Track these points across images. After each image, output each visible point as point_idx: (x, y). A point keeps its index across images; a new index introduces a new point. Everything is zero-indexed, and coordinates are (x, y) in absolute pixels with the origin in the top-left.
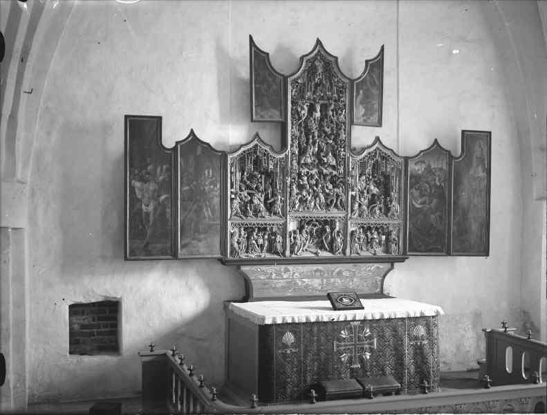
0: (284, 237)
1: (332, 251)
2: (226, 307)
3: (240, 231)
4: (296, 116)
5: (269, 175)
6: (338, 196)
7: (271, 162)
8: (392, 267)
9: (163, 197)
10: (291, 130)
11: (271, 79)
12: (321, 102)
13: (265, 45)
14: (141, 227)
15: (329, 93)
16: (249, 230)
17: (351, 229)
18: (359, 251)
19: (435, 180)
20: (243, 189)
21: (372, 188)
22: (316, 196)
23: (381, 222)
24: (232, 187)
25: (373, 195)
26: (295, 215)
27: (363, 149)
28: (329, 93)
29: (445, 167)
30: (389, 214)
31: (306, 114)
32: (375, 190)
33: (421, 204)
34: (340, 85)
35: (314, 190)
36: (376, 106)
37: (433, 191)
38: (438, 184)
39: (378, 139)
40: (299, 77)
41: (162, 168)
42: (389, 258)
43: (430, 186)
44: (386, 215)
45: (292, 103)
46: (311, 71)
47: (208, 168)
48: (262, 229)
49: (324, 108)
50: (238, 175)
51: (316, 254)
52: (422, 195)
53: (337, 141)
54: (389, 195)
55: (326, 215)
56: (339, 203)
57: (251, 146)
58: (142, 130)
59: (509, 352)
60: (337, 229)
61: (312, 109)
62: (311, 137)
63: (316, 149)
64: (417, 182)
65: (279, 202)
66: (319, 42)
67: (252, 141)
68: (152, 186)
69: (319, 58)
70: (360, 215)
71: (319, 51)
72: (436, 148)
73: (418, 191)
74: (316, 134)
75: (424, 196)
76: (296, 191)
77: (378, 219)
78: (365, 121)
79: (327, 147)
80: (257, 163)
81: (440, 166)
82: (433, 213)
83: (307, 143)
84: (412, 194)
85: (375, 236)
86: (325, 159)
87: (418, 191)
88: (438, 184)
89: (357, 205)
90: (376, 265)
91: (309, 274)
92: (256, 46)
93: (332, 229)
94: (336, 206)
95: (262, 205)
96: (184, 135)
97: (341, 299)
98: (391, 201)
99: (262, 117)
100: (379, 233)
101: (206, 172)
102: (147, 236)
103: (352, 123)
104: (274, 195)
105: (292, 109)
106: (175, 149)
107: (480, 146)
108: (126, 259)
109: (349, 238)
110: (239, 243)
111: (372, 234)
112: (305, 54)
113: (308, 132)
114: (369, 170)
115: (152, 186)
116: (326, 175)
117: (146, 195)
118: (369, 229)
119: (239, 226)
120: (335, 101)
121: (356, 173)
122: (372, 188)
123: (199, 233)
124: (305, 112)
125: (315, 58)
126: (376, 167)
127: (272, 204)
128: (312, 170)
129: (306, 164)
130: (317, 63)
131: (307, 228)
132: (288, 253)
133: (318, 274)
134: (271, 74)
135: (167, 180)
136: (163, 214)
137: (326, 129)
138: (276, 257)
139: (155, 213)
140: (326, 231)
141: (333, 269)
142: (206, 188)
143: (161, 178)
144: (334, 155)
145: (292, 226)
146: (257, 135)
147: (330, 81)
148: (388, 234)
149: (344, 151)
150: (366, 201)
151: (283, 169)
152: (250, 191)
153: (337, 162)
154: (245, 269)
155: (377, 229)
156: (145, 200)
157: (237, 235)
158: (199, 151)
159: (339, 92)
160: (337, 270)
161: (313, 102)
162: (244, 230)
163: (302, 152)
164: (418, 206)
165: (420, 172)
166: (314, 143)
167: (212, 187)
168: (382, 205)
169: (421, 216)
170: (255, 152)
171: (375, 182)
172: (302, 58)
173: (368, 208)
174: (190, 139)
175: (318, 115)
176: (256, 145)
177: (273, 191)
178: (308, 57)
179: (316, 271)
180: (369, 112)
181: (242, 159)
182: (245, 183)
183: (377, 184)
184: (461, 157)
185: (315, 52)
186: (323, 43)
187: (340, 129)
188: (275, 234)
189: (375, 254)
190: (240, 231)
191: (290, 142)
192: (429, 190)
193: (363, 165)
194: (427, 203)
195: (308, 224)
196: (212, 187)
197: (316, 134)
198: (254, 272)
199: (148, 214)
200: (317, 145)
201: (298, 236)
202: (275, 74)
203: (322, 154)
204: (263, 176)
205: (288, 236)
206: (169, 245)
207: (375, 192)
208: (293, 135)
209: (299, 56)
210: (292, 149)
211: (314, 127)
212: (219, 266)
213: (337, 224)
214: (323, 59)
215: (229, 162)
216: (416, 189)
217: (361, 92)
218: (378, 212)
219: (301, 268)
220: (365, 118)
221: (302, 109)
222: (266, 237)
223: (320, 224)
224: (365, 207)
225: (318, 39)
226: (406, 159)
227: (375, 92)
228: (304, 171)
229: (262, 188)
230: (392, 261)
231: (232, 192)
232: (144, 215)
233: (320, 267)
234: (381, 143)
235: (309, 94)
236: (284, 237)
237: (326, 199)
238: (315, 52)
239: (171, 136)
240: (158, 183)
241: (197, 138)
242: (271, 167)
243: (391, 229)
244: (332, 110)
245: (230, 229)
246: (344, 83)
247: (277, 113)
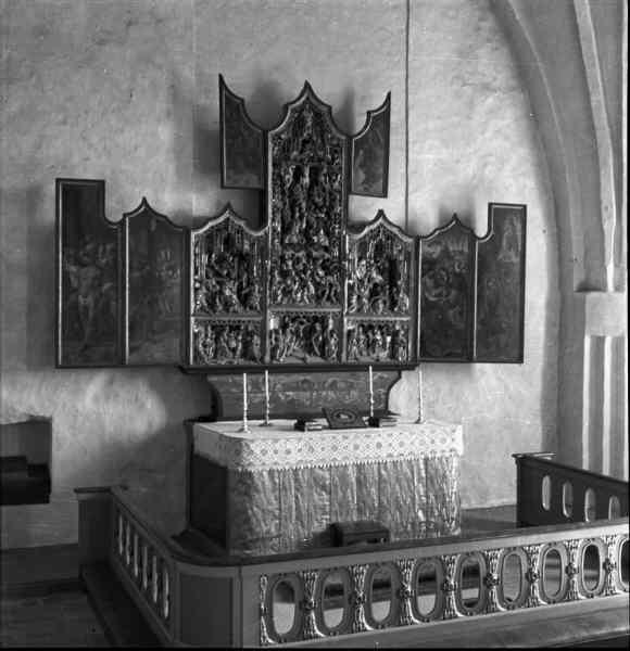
0: (263, 339)
1: (323, 355)
2: (190, 432)
3: (206, 330)
4: (279, 183)
5: (243, 258)
6: (331, 285)
7: (246, 241)
8: (400, 377)
9: (106, 286)
10: (272, 201)
11: (246, 133)
13: (241, 86)
14: (76, 325)
15: (321, 153)
16: (218, 330)
17: (348, 327)
18: (358, 356)
19: (453, 267)
20: (211, 275)
21: (374, 275)
22: (304, 286)
23: (388, 318)
24: (196, 273)
25: (376, 285)
26: (276, 310)
27: (363, 225)
28: (321, 153)
29: (466, 250)
30: (396, 309)
31: (291, 180)
32: (379, 278)
33: (435, 296)
34: (335, 142)
35: (301, 278)
36: (381, 171)
37: (451, 280)
38: (457, 270)
39: (381, 213)
40: (282, 132)
41: (104, 250)
42: (397, 366)
43: (447, 274)
44: (392, 309)
45: (274, 165)
46: (299, 124)
47: (164, 248)
48: (235, 328)
49: (315, 173)
50: (205, 258)
51: (304, 359)
52: (437, 286)
53: (330, 212)
54: (396, 285)
55: (316, 310)
56: (333, 293)
57: (221, 219)
58: (82, 198)
59: (546, 481)
60: (331, 327)
61: (298, 174)
62: (297, 209)
63: (304, 226)
64: (430, 270)
65: (256, 293)
66: (307, 86)
67: (222, 214)
68: (91, 272)
69: (307, 106)
70: (359, 310)
71: (308, 98)
72: (456, 225)
74: (304, 205)
75: (437, 286)
76: (278, 279)
77: (381, 315)
78: (365, 189)
79: (318, 224)
80: (228, 242)
81: (460, 248)
83: (293, 217)
84: (424, 284)
85: (378, 337)
86: (315, 238)
87: (432, 280)
89: (355, 297)
90: (379, 374)
91: (295, 385)
92: (226, 88)
93: (324, 328)
94: (329, 298)
95: (235, 297)
96: (134, 205)
97: (338, 416)
98: (398, 292)
99: (235, 182)
100: (382, 334)
101: (163, 253)
102: (83, 341)
103: (349, 191)
104: (250, 283)
105: (273, 174)
106: (123, 221)
108: (57, 367)
109: (345, 340)
110: (205, 346)
111: (374, 334)
113: (294, 204)
114: (371, 251)
115: (91, 272)
116: (315, 260)
117: (84, 283)
118: (371, 327)
119: (205, 324)
120: (328, 164)
121: (354, 256)
122: (374, 275)
123: (154, 332)
124: (289, 177)
125: (302, 109)
126: (379, 248)
127: (248, 296)
128: (298, 251)
129: (291, 244)
130: (305, 113)
131: (292, 327)
132: (267, 358)
133: (305, 386)
135: (111, 262)
136: (107, 305)
137: (317, 200)
138: (252, 363)
139: (96, 306)
140: (315, 331)
141: (323, 380)
142: (163, 274)
143: (104, 261)
144: (327, 234)
145: (272, 324)
146: (228, 206)
147: (322, 136)
148: (395, 334)
149: (340, 228)
150: (367, 292)
151: (263, 252)
152: (220, 279)
154: (213, 379)
155: (380, 328)
156: (83, 290)
157: (203, 335)
158: (154, 226)
159: (334, 152)
160: (330, 381)
162: (212, 329)
163: (286, 229)
164: (432, 299)
165: (435, 256)
166: (301, 218)
167: (170, 273)
168: (386, 298)
169: (435, 312)
170: (227, 229)
171: (378, 268)
172: (286, 107)
173: (369, 300)
174: (142, 209)
175: (307, 180)
176: (228, 219)
177: (249, 279)
178: (294, 105)
179: (305, 381)
180: (370, 179)
181: (209, 237)
182: (212, 268)
183: (380, 272)
184: (486, 236)
185: (303, 99)
186: (313, 87)
187: (334, 200)
188: (249, 334)
189: (378, 360)
190: (206, 330)
191: (270, 216)
193: (363, 246)
195: (293, 320)
196: (170, 273)
197: (304, 205)
198: (222, 384)
199: (86, 308)
201: (281, 337)
202: (252, 127)
203: (311, 232)
204: (236, 259)
205: (267, 337)
206: (113, 349)
207: (377, 281)
208: (274, 206)
209: (282, 104)
210: (273, 224)
211: (301, 196)
212: (178, 377)
213: (331, 321)
214: (313, 108)
215: (193, 240)
216: (430, 278)
217: (361, 152)
218: (381, 306)
219: (284, 379)
221: (287, 172)
222: (240, 338)
223: (308, 321)
224: (365, 300)
226: (418, 239)
227: (381, 153)
228: (289, 253)
229: (234, 275)
230: (396, 369)
231: (195, 280)
232: (81, 310)
233: (308, 377)
234: (385, 218)
235: (295, 153)
236: (263, 339)
237: (316, 290)
238: (303, 99)
239: (114, 210)
240: (100, 268)
241: (151, 209)
242: (247, 247)
243: (397, 327)
244: (325, 176)
245: (194, 328)
246: (339, 139)
247: (255, 178)
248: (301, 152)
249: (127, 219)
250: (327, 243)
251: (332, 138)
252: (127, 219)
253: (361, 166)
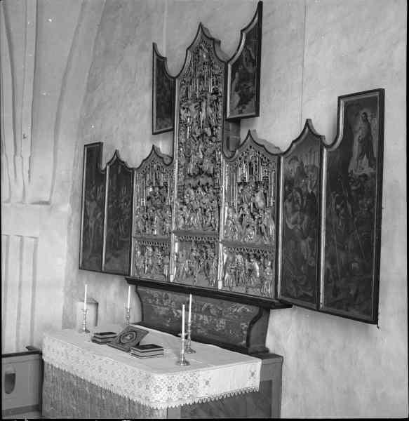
73: (291, 203)
82: (304, 238)
87: (291, 203)
88: (310, 191)
107: (366, 120)
142: (122, 205)
154: (140, 289)
160: (205, 306)
192: (300, 202)
194: (299, 220)
217: (237, 75)
220: (241, 108)
225: (201, 23)
249: (108, 167)
252: (108, 167)
253: (236, 90)
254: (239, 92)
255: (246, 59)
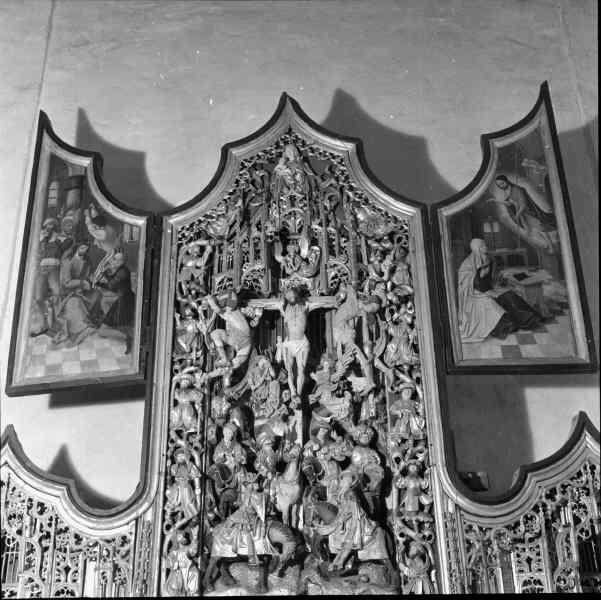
11: (99, 234)
12: (313, 304)
69: (290, 152)
112: (230, 141)
134: (103, 219)
144: (378, 514)
153: (390, 545)
161: (276, 304)
166: (280, 467)
175: (293, 346)
200: (291, 471)
217: (476, 245)
225: (284, 98)
247: (119, 350)
248: (276, 271)
250: (375, 551)
251: (373, 222)
254: (499, 291)
255: (512, 209)
